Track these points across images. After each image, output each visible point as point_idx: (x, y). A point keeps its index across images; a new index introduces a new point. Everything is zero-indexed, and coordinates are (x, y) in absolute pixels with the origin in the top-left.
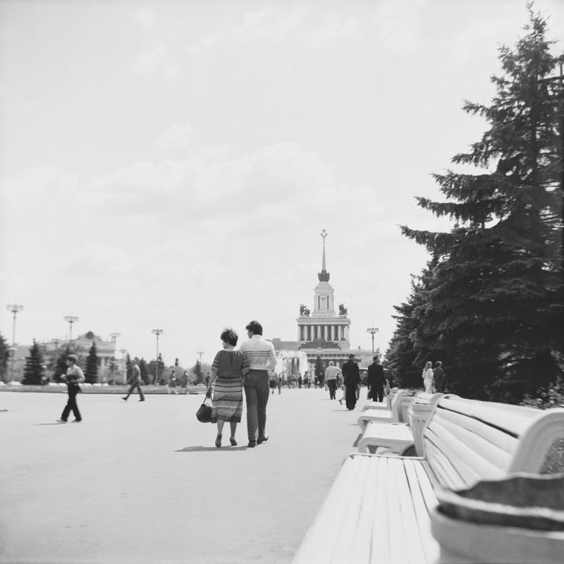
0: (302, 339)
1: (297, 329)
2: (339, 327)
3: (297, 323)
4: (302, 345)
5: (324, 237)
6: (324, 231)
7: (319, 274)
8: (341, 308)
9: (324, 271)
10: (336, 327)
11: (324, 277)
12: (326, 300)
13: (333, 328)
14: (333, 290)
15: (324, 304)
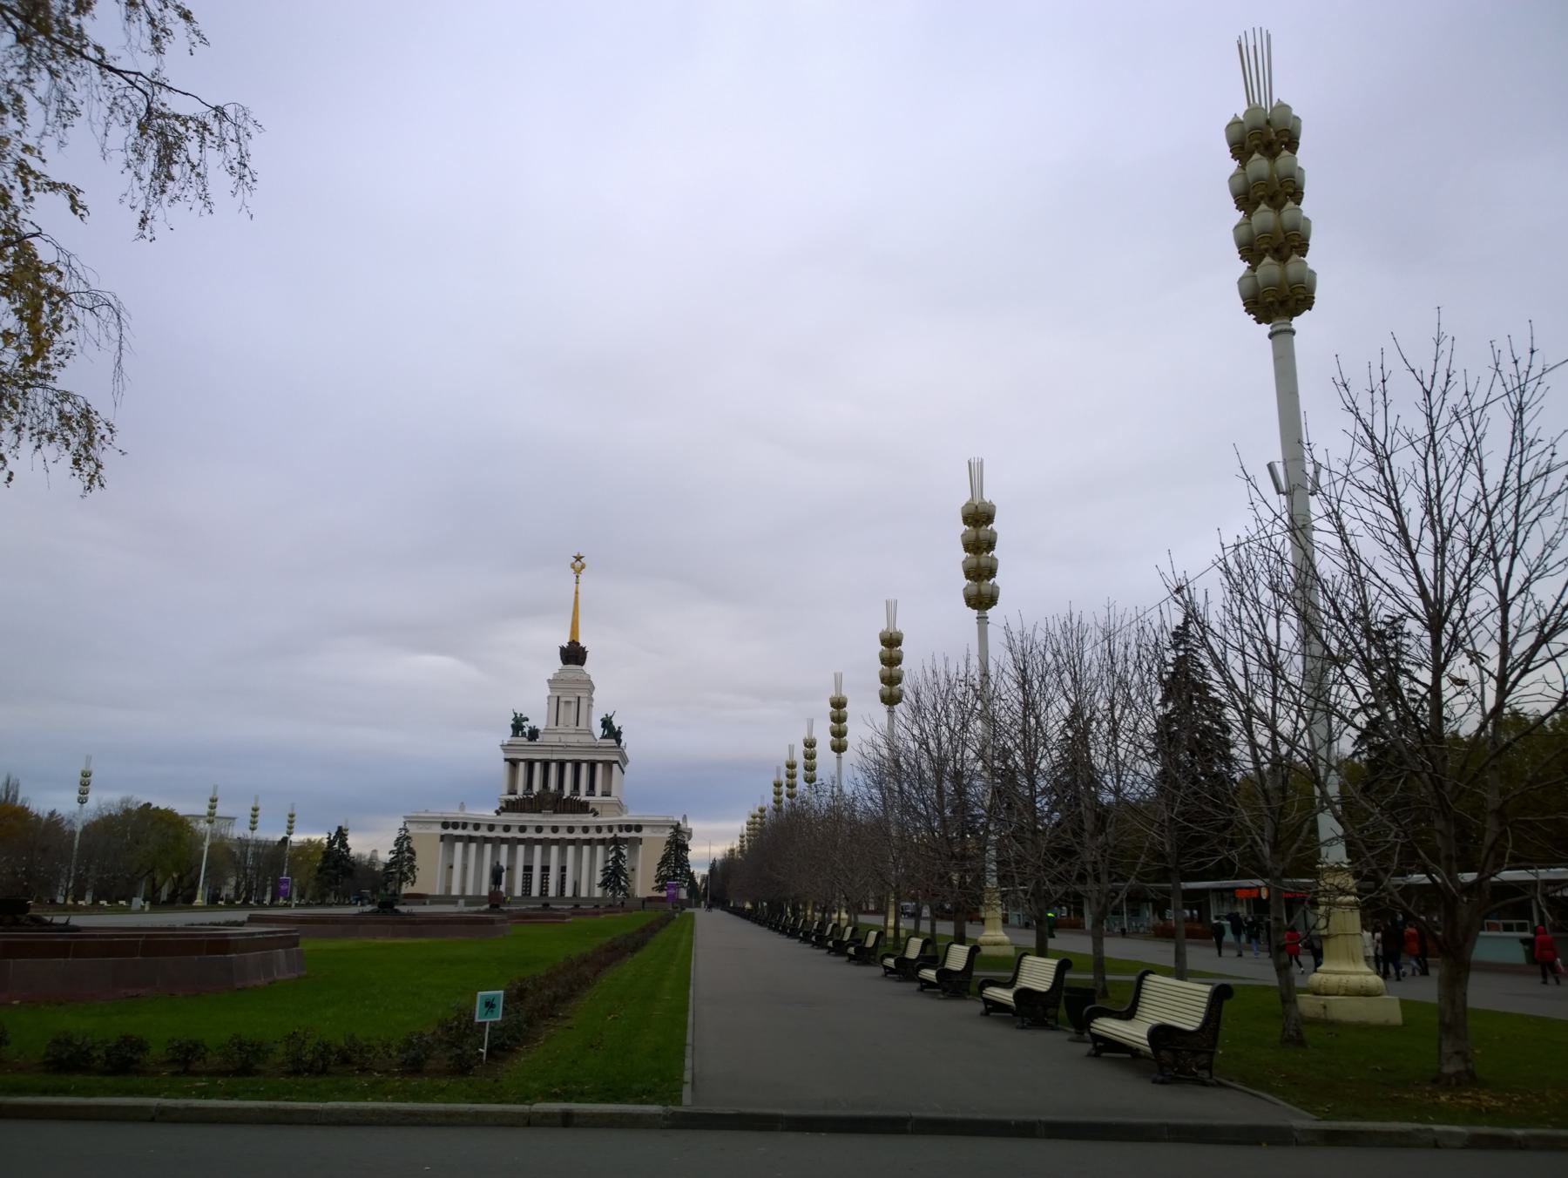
0: (513, 792)
1: (504, 768)
2: (600, 767)
3: (502, 755)
4: (508, 802)
5: (578, 572)
6: (578, 558)
7: (562, 649)
8: (607, 723)
9: (574, 644)
10: (592, 765)
11: (573, 654)
12: (574, 707)
13: (584, 767)
14: (589, 682)
15: (568, 714)
